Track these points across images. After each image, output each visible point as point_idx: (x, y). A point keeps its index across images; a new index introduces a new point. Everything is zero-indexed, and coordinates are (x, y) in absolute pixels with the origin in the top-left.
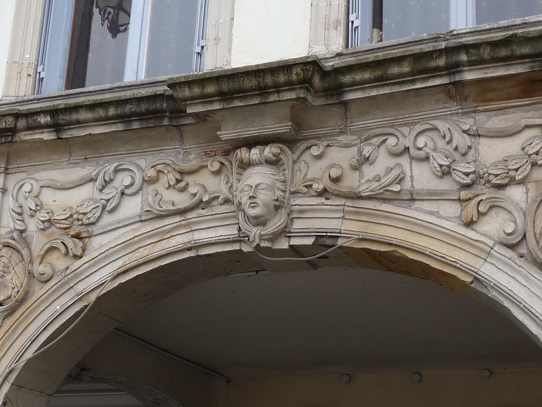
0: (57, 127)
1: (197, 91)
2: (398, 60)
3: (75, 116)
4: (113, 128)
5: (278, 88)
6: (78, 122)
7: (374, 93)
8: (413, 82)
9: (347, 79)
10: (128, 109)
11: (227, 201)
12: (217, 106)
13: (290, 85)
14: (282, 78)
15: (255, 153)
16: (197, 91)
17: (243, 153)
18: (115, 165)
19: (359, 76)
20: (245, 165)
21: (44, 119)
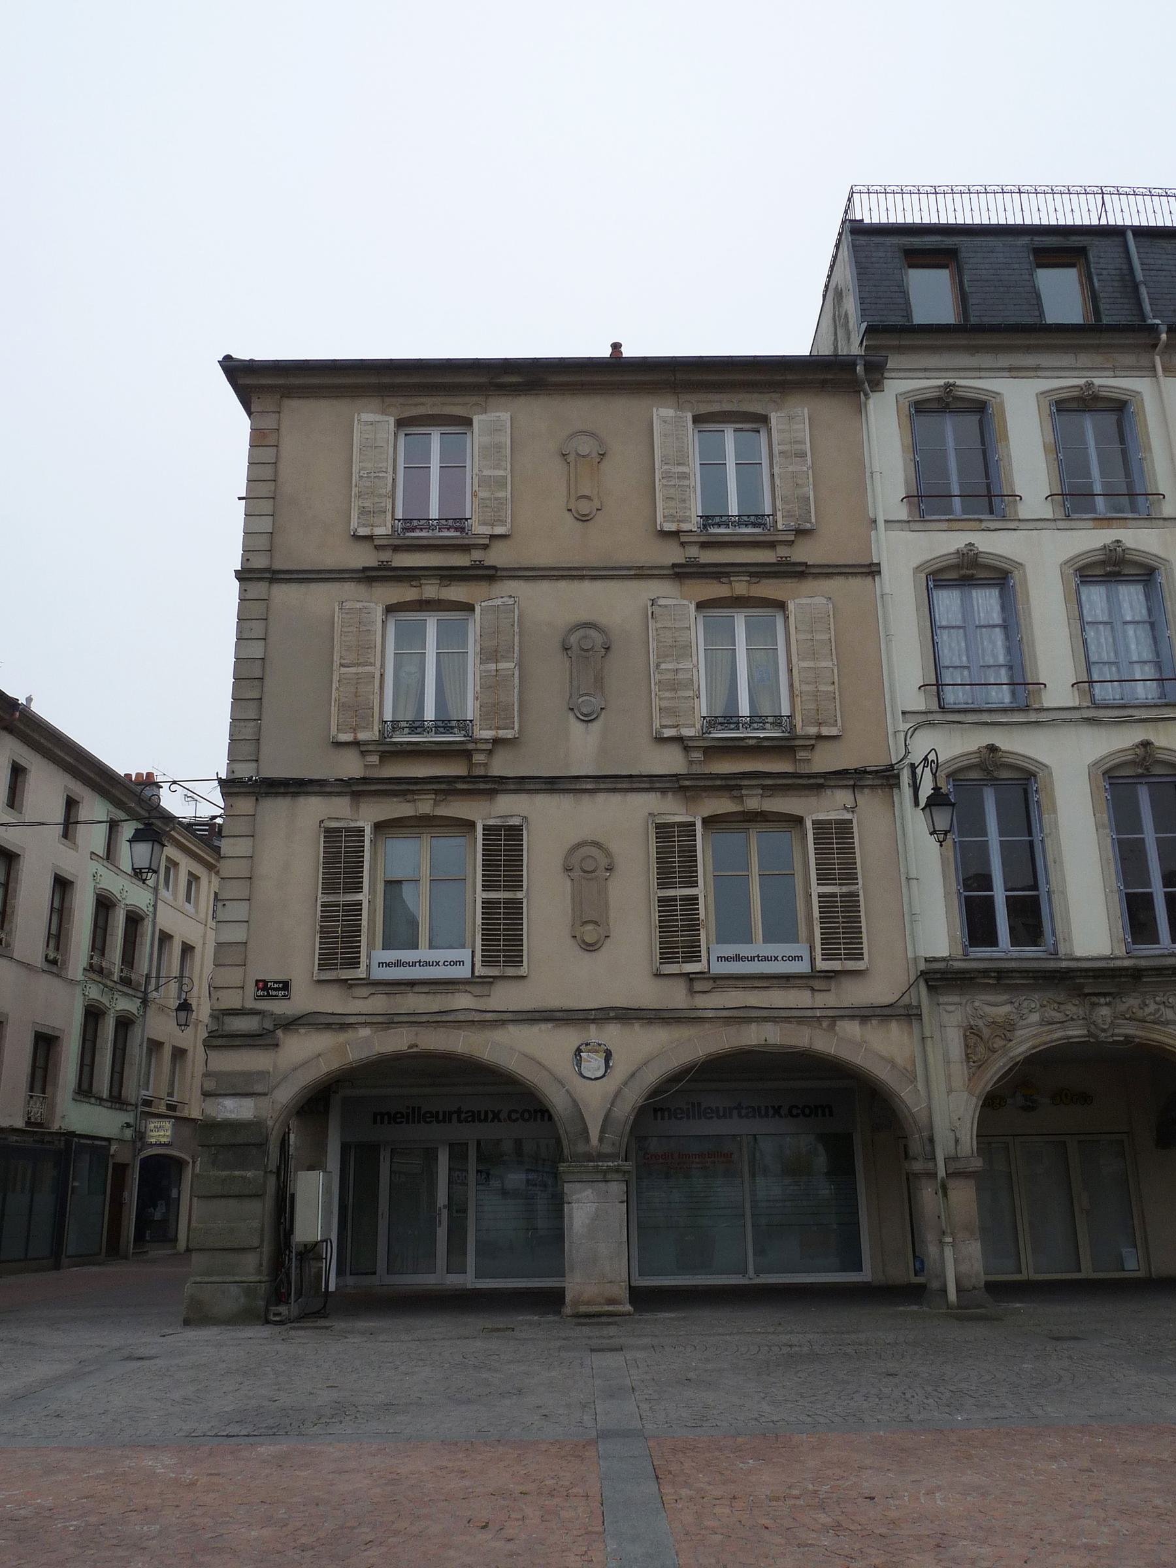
0: (998, 978)
1: (1083, 974)
2: (1168, 969)
3: (1010, 975)
4: (1028, 982)
5: (1120, 976)
6: (1012, 977)
7: (1155, 979)
8: (1171, 977)
9: (1145, 973)
10: (1039, 974)
11: (1083, 1018)
12: (1091, 981)
13: (1126, 976)
14: (1124, 973)
15: (1102, 1000)
16: (1083, 974)
17: (1095, 999)
18: (1024, 997)
19: (1150, 973)
20: (1094, 1005)
21: (993, 974)
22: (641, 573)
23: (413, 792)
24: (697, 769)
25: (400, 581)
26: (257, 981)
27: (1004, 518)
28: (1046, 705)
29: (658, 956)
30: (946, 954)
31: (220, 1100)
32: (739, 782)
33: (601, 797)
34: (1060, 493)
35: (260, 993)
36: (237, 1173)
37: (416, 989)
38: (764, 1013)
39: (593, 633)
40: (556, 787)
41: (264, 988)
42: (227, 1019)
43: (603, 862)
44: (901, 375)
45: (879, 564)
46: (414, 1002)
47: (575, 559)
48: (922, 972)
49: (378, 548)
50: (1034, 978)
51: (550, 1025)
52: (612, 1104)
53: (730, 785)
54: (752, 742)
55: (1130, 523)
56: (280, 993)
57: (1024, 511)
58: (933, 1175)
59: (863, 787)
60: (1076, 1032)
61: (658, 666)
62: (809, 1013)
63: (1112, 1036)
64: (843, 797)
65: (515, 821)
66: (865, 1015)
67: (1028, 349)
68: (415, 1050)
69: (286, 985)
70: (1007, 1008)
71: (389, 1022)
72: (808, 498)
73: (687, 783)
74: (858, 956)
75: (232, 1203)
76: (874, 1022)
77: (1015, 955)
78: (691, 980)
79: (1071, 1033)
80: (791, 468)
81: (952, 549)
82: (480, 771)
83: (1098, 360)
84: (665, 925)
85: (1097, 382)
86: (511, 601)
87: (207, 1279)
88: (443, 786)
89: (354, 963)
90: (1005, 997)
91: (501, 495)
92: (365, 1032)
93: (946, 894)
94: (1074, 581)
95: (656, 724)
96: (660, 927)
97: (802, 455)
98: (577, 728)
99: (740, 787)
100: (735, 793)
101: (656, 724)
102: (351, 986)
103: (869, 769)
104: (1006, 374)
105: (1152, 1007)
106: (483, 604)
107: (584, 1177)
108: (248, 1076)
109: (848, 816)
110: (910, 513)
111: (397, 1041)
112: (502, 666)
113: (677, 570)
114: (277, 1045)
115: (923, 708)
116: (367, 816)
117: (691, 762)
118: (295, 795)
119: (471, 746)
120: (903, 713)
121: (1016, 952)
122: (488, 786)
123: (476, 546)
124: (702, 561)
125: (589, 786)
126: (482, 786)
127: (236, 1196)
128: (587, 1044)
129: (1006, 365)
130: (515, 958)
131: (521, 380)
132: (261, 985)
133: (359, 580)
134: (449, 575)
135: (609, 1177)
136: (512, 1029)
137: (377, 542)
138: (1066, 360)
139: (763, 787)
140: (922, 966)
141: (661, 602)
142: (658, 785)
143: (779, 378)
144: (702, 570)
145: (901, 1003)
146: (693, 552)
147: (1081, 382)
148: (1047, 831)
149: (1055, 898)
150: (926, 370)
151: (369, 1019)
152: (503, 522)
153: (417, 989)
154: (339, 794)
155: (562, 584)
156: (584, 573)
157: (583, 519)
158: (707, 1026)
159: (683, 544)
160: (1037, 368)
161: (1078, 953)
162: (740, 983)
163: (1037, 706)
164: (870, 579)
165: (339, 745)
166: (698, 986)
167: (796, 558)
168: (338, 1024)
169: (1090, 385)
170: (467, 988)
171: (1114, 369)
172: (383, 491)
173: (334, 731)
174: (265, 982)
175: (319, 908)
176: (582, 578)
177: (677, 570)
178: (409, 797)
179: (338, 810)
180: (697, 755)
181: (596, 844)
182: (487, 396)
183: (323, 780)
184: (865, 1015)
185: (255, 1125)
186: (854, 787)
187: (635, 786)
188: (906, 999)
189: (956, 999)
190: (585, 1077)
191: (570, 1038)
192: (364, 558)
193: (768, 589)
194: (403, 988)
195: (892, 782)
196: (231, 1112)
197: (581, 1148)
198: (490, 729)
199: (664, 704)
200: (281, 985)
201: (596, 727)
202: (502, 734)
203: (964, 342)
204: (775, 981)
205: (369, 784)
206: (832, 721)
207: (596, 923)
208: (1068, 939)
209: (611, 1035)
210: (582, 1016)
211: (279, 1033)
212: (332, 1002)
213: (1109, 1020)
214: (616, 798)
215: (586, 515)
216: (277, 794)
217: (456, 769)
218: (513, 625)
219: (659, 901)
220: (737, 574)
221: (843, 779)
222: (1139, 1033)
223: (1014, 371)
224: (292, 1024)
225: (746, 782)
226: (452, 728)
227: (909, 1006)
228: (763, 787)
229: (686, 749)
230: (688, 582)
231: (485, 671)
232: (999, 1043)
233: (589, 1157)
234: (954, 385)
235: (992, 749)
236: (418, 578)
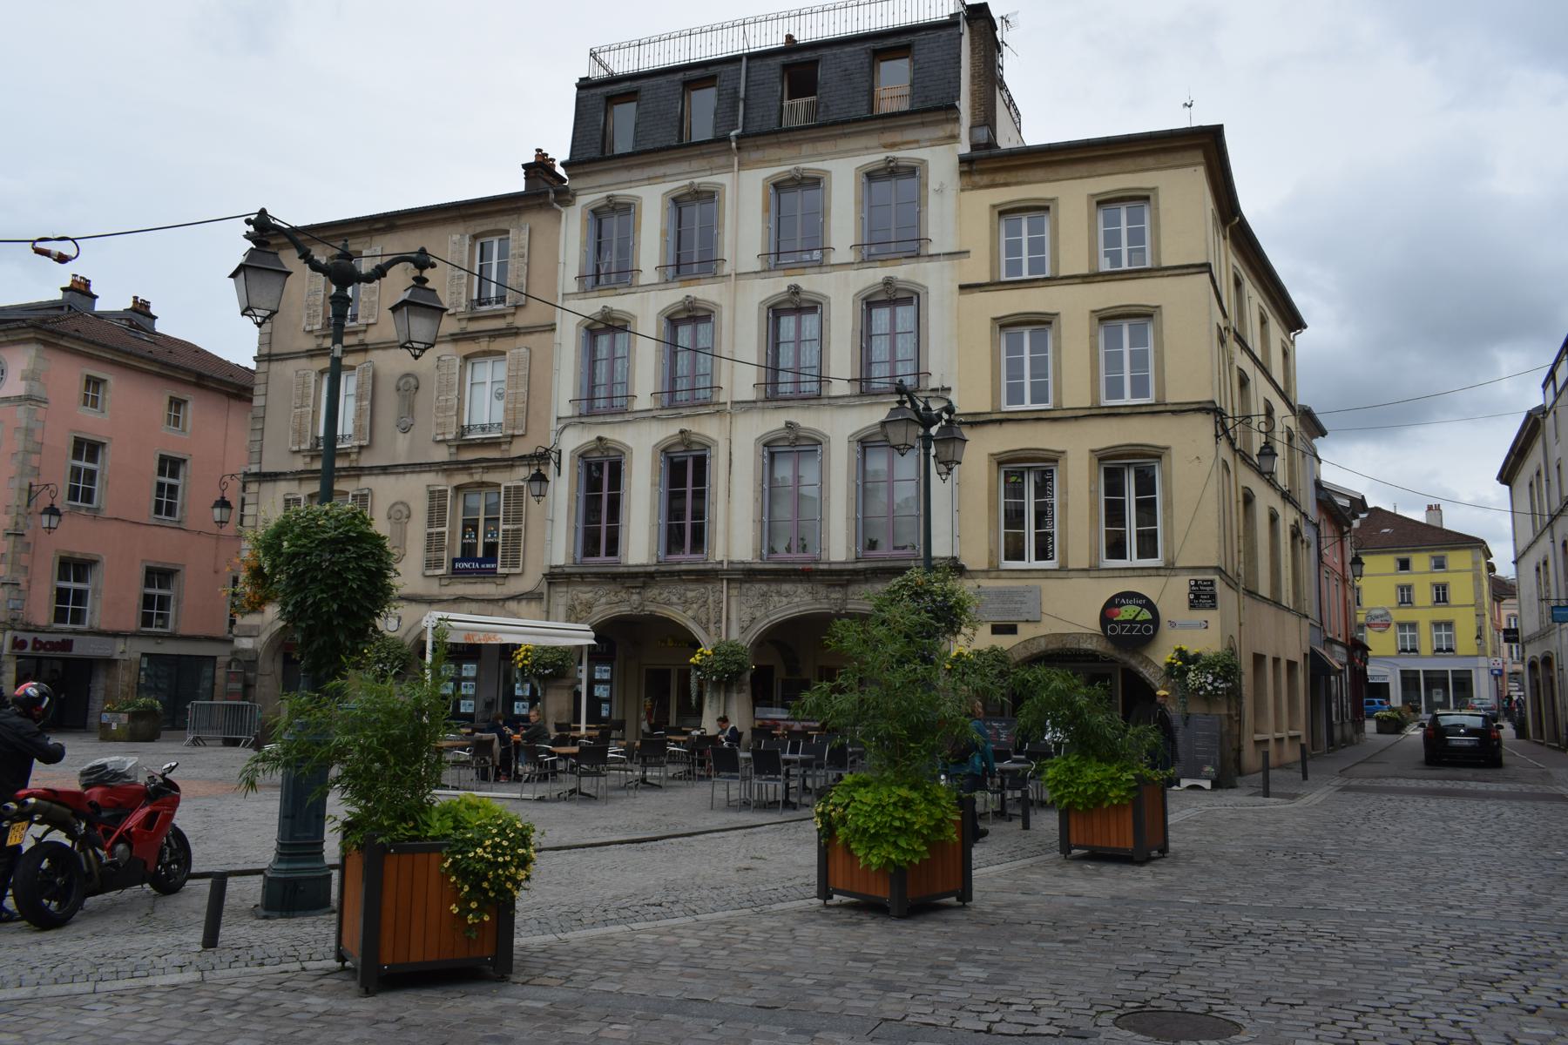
0: (582, 578)
17: (631, 590)
20: (632, 593)
24: (454, 458)
30: (562, 563)
33: (408, 476)
34: (682, 261)
43: (405, 512)
44: (586, 191)
48: (544, 575)
49: (317, 336)
53: (466, 466)
55: (702, 281)
57: (643, 279)
60: (624, 609)
61: (438, 398)
63: (643, 610)
65: (366, 492)
67: (661, 162)
70: (590, 595)
73: (445, 467)
74: (516, 565)
82: (354, 465)
83: (703, 163)
85: (697, 181)
90: (589, 589)
93: (568, 528)
98: (401, 436)
99: (471, 468)
101: (433, 433)
104: (647, 182)
105: (665, 595)
109: (522, 484)
115: (570, 414)
118: (275, 481)
119: (349, 451)
120: (559, 418)
124: (469, 329)
126: (352, 473)
129: (645, 176)
133: (307, 357)
138: (684, 166)
139: (483, 468)
141: (443, 358)
143: (514, 206)
145: (538, 591)
146: (464, 324)
147: (687, 182)
150: (600, 186)
152: (373, 316)
154: (293, 479)
160: (665, 176)
161: (631, 562)
169: (692, 184)
171: (711, 169)
180: (453, 450)
181: (402, 503)
182: (371, 237)
185: (254, 651)
186: (529, 465)
189: (565, 589)
193: (497, 345)
201: (408, 435)
203: (620, 165)
213: (637, 602)
220: (483, 337)
223: (651, 180)
225: (473, 465)
229: (450, 446)
230: (460, 344)
234: (613, 196)
235: (600, 439)
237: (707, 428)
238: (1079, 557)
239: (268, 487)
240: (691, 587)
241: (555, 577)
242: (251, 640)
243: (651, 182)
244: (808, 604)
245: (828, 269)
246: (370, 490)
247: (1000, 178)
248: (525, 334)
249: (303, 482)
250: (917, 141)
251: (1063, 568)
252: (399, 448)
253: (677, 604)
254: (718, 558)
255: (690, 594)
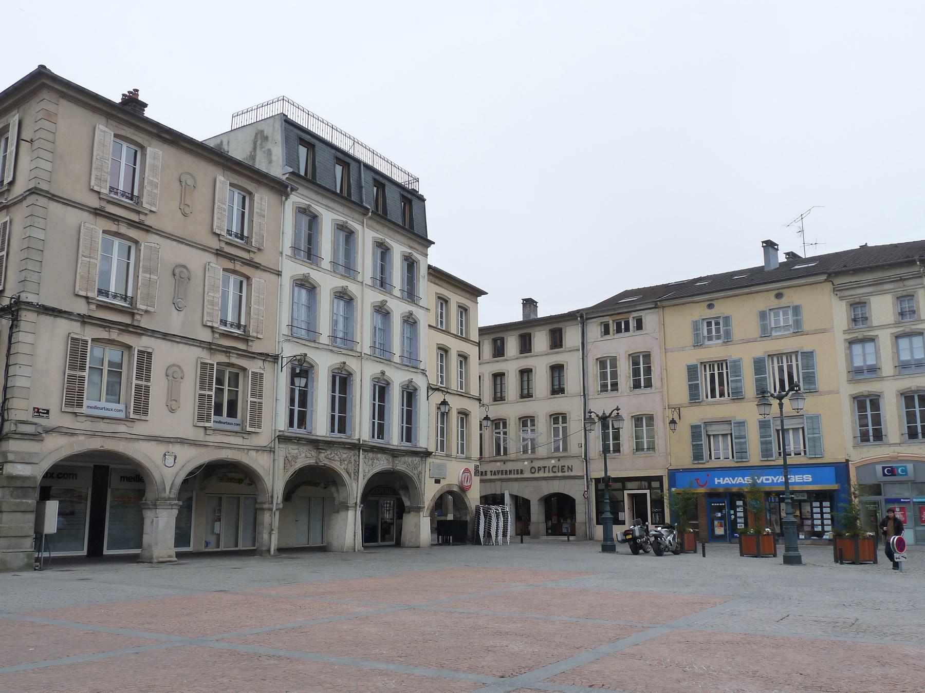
0: (298, 441)
22: (205, 249)
23: (110, 327)
24: (215, 341)
25: (109, 219)
26: (34, 408)
27: (317, 265)
28: (320, 342)
29: (197, 418)
31: (15, 465)
32: (230, 350)
33: (181, 345)
35: (36, 414)
36: (24, 501)
37: (105, 421)
38: (228, 446)
39: (185, 270)
40: (166, 338)
41: (37, 411)
42: (19, 425)
43: (181, 375)
45: (281, 272)
46: (103, 426)
47: (178, 232)
50: (308, 441)
51: (155, 443)
52: (175, 478)
53: (227, 351)
54: (236, 335)
56: (45, 415)
58: (271, 510)
59: (267, 361)
61: (208, 293)
62: (242, 447)
64: (259, 363)
66: (258, 449)
68: (102, 448)
69: (48, 412)
70: (297, 451)
71: (93, 435)
72: (264, 236)
73: (214, 347)
75: (19, 515)
76: (260, 452)
77: (297, 432)
78: (206, 429)
79: (311, 462)
80: (259, 221)
81: (302, 273)
82: (136, 324)
84: (201, 406)
86: (158, 247)
87: (8, 551)
88: (123, 328)
89: (80, 405)
90: (297, 447)
91: (155, 191)
92: (82, 438)
94: (333, 296)
95: (205, 319)
96: (199, 406)
97: (264, 216)
100: (228, 354)
102: (77, 415)
103: (270, 354)
106: (145, 244)
107: (167, 507)
108: (30, 454)
110: (291, 253)
111: (96, 444)
112: (152, 276)
113: (218, 252)
114: (43, 440)
116: (89, 333)
117: (214, 338)
118: (56, 316)
119: (136, 311)
121: (299, 431)
122: (141, 332)
123: (143, 213)
125: (178, 340)
127: (22, 512)
128: (168, 452)
130: (146, 413)
131: (170, 138)
132: (36, 410)
133: (90, 212)
134: (132, 224)
135: (173, 507)
136: (141, 442)
137: (101, 196)
139: (237, 354)
140: (278, 434)
141: (211, 264)
142: (202, 345)
144: (226, 255)
146: (223, 245)
147: (345, 220)
148: (315, 388)
149: (314, 413)
150: (303, 195)
151: (85, 432)
153: (105, 421)
154: (75, 320)
155: (175, 243)
156: (184, 241)
157: (185, 215)
158: (209, 449)
159: (219, 240)
162: (222, 433)
163: (318, 341)
164: (277, 276)
165: (78, 295)
166: (208, 432)
167: (256, 260)
168: (71, 433)
170: (125, 423)
172: (106, 170)
173: (77, 289)
174: (38, 409)
175: (66, 377)
176: (182, 243)
177: (218, 252)
178: (107, 329)
179: (74, 328)
181: (179, 367)
183: (70, 312)
184: (258, 449)
186: (264, 360)
187: (195, 344)
188: (270, 445)
190: (166, 466)
191: (161, 449)
192: (94, 202)
194: (99, 419)
195: (276, 361)
196: (20, 471)
197: (163, 495)
198: (144, 305)
199: (209, 311)
200: (45, 411)
202: (149, 309)
203: (316, 189)
204: (233, 433)
205: (92, 319)
206: (261, 332)
207: (176, 401)
208: (315, 429)
209: (177, 449)
210: (167, 440)
211: (44, 435)
212: (68, 422)
214: (187, 347)
215: (185, 213)
216: (47, 314)
217: (126, 320)
218: (158, 259)
219: (199, 395)
220: (238, 261)
221: (262, 356)
222: (328, 463)
224: (50, 431)
226: (103, 293)
227: (271, 448)
228: (237, 354)
229: (213, 332)
231: (144, 277)
232: (293, 463)
233: (165, 499)
236: (118, 221)
237: (353, 364)
238: (454, 453)
239: (46, 321)
240: (345, 452)
241: (283, 439)
242: (29, 467)
243: (327, 208)
244: (386, 465)
245: (392, 297)
246: (153, 349)
247: (437, 281)
248: (261, 269)
249: (86, 325)
250: (418, 250)
251: (449, 456)
252: (175, 323)
253: (338, 461)
254: (357, 437)
255: (345, 456)
